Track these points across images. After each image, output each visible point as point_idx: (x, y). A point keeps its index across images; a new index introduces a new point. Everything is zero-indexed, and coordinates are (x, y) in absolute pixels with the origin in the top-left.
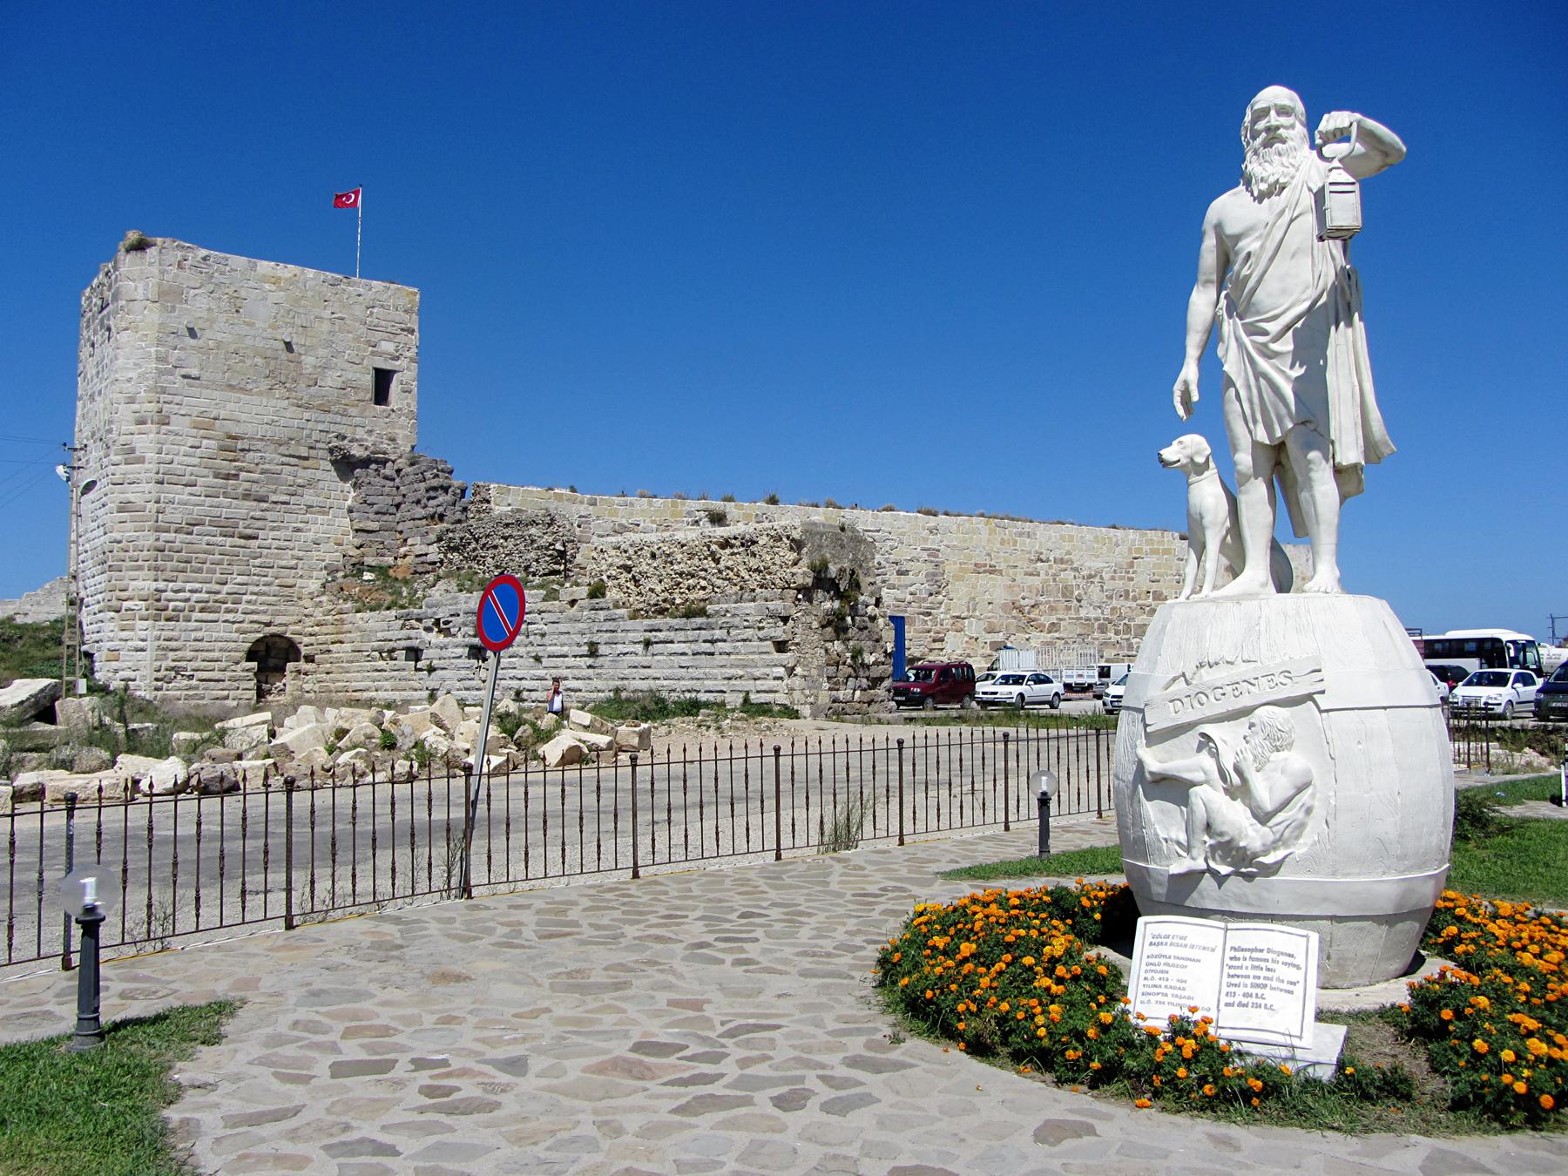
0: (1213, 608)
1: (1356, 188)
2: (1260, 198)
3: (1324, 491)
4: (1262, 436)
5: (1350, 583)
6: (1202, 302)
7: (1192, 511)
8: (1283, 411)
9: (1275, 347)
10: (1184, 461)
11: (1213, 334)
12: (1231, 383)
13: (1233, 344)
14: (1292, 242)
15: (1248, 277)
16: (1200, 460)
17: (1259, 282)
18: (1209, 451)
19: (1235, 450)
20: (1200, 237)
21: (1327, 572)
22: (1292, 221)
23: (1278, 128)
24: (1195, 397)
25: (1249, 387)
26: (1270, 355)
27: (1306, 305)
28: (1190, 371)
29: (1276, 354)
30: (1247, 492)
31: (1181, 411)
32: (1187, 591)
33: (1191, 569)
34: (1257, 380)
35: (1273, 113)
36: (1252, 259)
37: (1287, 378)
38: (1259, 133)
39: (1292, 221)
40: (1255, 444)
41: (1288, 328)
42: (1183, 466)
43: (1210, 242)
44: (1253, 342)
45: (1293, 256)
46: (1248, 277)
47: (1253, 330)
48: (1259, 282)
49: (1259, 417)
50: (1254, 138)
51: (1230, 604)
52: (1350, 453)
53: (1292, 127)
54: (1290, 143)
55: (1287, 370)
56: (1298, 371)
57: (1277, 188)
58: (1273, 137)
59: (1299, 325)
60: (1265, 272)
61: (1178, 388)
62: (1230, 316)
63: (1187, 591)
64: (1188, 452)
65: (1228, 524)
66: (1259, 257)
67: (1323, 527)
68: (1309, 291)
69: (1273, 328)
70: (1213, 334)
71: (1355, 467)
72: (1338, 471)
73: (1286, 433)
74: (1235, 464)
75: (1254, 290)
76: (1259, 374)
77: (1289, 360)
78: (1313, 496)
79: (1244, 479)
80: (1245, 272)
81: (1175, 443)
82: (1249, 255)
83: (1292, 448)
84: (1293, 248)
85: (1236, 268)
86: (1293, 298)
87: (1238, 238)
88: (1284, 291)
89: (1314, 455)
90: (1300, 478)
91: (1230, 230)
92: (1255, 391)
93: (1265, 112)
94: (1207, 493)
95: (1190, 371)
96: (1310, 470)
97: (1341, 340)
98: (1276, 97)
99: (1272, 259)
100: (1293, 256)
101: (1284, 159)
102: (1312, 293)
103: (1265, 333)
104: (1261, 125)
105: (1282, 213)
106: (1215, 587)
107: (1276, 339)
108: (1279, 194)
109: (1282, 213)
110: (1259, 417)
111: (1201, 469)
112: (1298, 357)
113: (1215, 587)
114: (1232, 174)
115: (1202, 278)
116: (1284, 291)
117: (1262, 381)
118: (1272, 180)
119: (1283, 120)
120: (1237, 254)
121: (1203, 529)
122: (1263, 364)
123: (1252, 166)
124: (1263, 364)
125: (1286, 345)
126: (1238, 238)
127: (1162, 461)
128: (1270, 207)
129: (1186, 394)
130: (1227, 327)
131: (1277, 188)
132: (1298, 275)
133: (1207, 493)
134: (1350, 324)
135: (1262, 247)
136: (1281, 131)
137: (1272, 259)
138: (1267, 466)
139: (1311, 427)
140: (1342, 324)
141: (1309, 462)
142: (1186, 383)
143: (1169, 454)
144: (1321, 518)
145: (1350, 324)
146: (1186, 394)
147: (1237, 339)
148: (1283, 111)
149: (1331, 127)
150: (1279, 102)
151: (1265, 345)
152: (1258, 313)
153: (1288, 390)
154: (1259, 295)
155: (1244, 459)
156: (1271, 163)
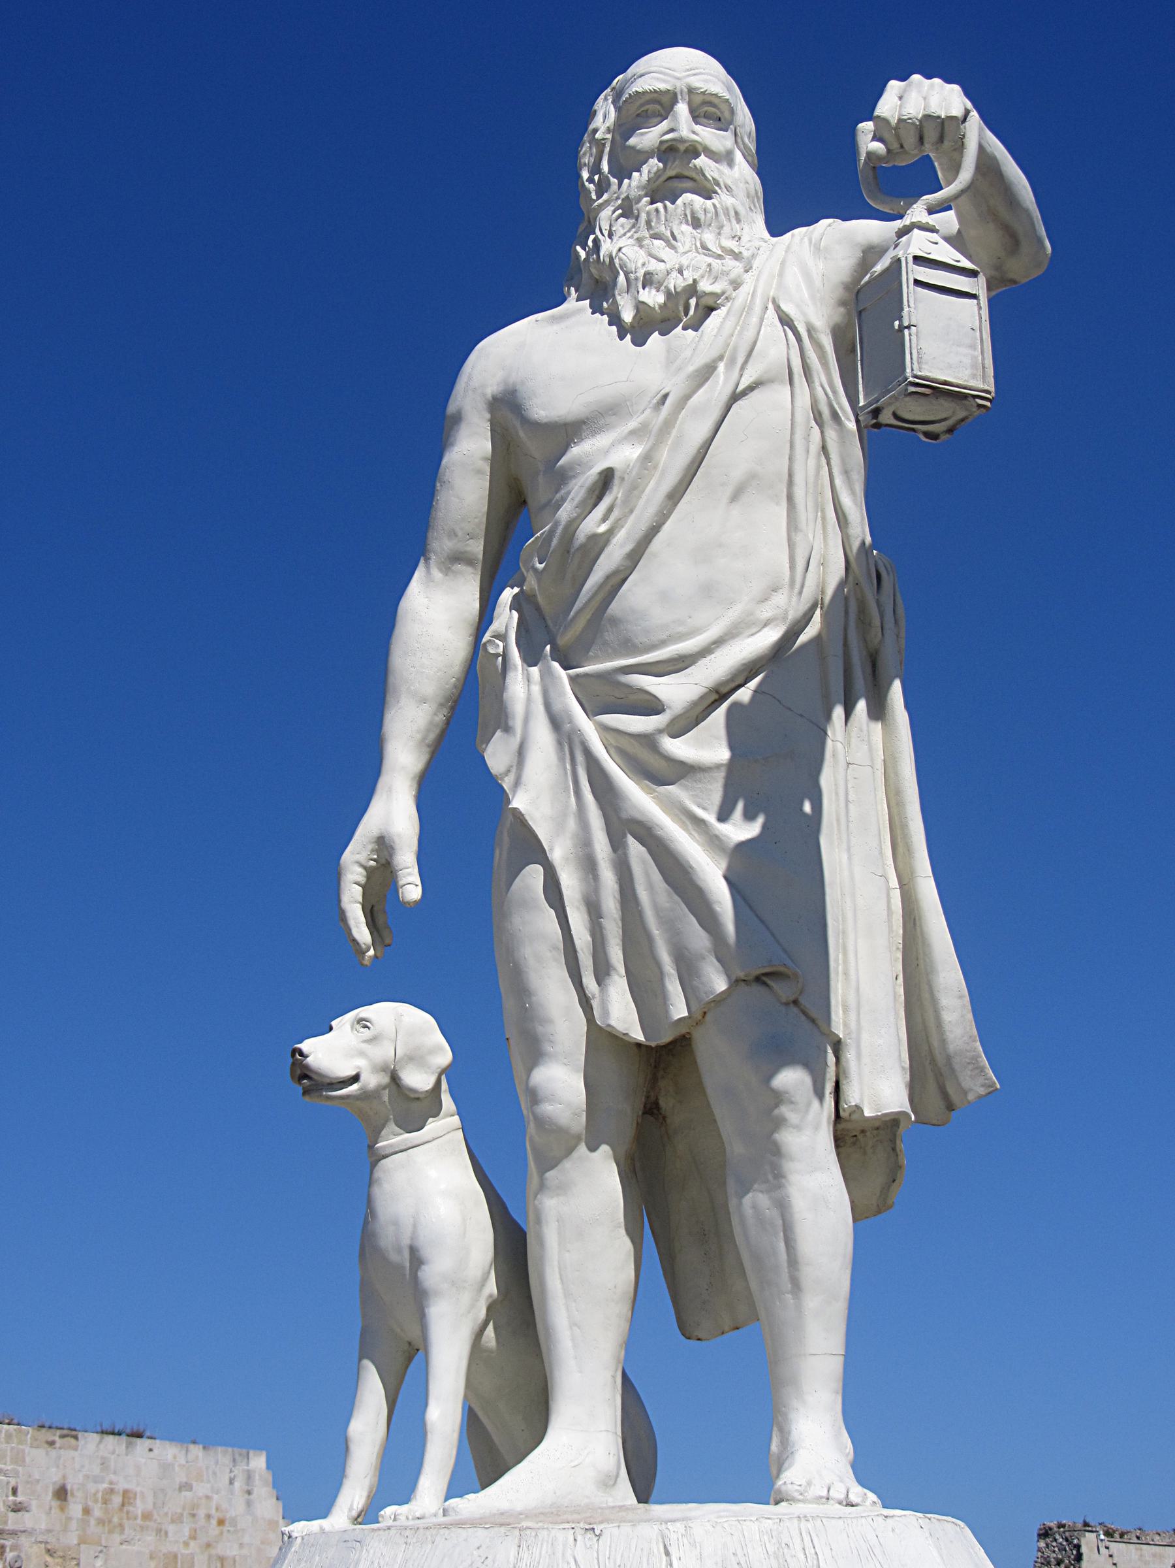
0: (506, 1549)
1: (978, 286)
2: (640, 330)
3: (816, 1194)
4: (622, 1013)
5: (893, 1470)
6: (436, 616)
7: (387, 1238)
8: (698, 938)
9: (679, 748)
10: (371, 1080)
11: (473, 705)
12: (531, 849)
13: (542, 738)
14: (734, 455)
15: (598, 543)
16: (419, 1080)
17: (635, 557)
18: (445, 1057)
19: (535, 1053)
20: (438, 430)
21: (817, 1440)
22: (735, 397)
23: (694, 151)
24: (412, 891)
25: (589, 866)
26: (662, 772)
27: (770, 636)
28: (393, 810)
29: (683, 771)
30: (563, 1189)
31: (362, 934)
32: (353, 1495)
33: (368, 1425)
34: (617, 844)
35: (682, 108)
36: (616, 493)
37: (714, 842)
38: (638, 160)
39: (735, 397)
40: (602, 1040)
41: (718, 695)
42: (366, 1096)
43: (470, 451)
44: (604, 729)
45: (735, 497)
46: (598, 543)
47: (607, 697)
48: (635, 557)
49: (616, 955)
50: (622, 172)
51: (561, 1535)
52: (880, 1085)
53: (726, 158)
54: (723, 199)
55: (710, 818)
56: (740, 830)
57: (689, 308)
58: (678, 173)
59: (744, 694)
60: (653, 531)
61: (355, 860)
62: (531, 658)
63: (353, 1495)
64: (384, 1052)
65: (492, 1288)
66: (635, 489)
67: (812, 1302)
68: (780, 599)
69: (678, 691)
70: (473, 705)
71: (891, 1124)
72: (853, 1138)
73: (705, 1010)
74: (534, 1097)
75: (617, 581)
76: (623, 826)
77: (716, 794)
78: (783, 1206)
79: (556, 1147)
80: (593, 524)
81: (343, 1024)
82: (606, 479)
83: (719, 1061)
84: (737, 475)
85: (565, 513)
86: (732, 615)
87: (570, 431)
88: (708, 591)
89: (791, 1078)
90: (736, 1148)
91: (549, 404)
92: (608, 877)
93: (659, 105)
94: (432, 1187)
95: (393, 810)
96: (779, 1123)
97: (859, 754)
98: (692, 71)
99: (675, 496)
100: (735, 497)
101: (709, 237)
102: (787, 604)
103: (650, 706)
104: (648, 137)
105: (706, 373)
106: (455, 1489)
107: (679, 728)
108: (696, 326)
109: (706, 373)
110: (616, 955)
111: (414, 1110)
112: (742, 786)
113: (455, 1489)
114: (545, 262)
115: (441, 544)
116: (708, 591)
117: (635, 848)
118: (676, 282)
119: (706, 135)
120: (562, 478)
121: (418, 1298)
122: (639, 797)
123: (619, 242)
124: (639, 797)
125: (708, 746)
126: (570, 431)
127: (305, 1076)
128: (671, 358)
129: (382, 875)
130: (522, 687)
131: (689, 308)
132: (743, 542)
133: (432, 1187)
134: (878, 711)
135: (647, 458)
136: (702, 161)
137: (675, 496)
138: (624, 1110)
139: (783, 990)
140: (861, 706)
141: (779, 1098)
142: (384, 846)
143: (334, 1051)
144: (808, 1274)
145: (878, 711)
146: (382, 875)
147: (557, 722)
148: (707, 110)
149: (914, 109)
150: (697, 82)
151: (648, 740)
152: (629, 646)
153: (712, 874)
154: (636, 595)
155: (562, 1083)
156: (671, 241)
